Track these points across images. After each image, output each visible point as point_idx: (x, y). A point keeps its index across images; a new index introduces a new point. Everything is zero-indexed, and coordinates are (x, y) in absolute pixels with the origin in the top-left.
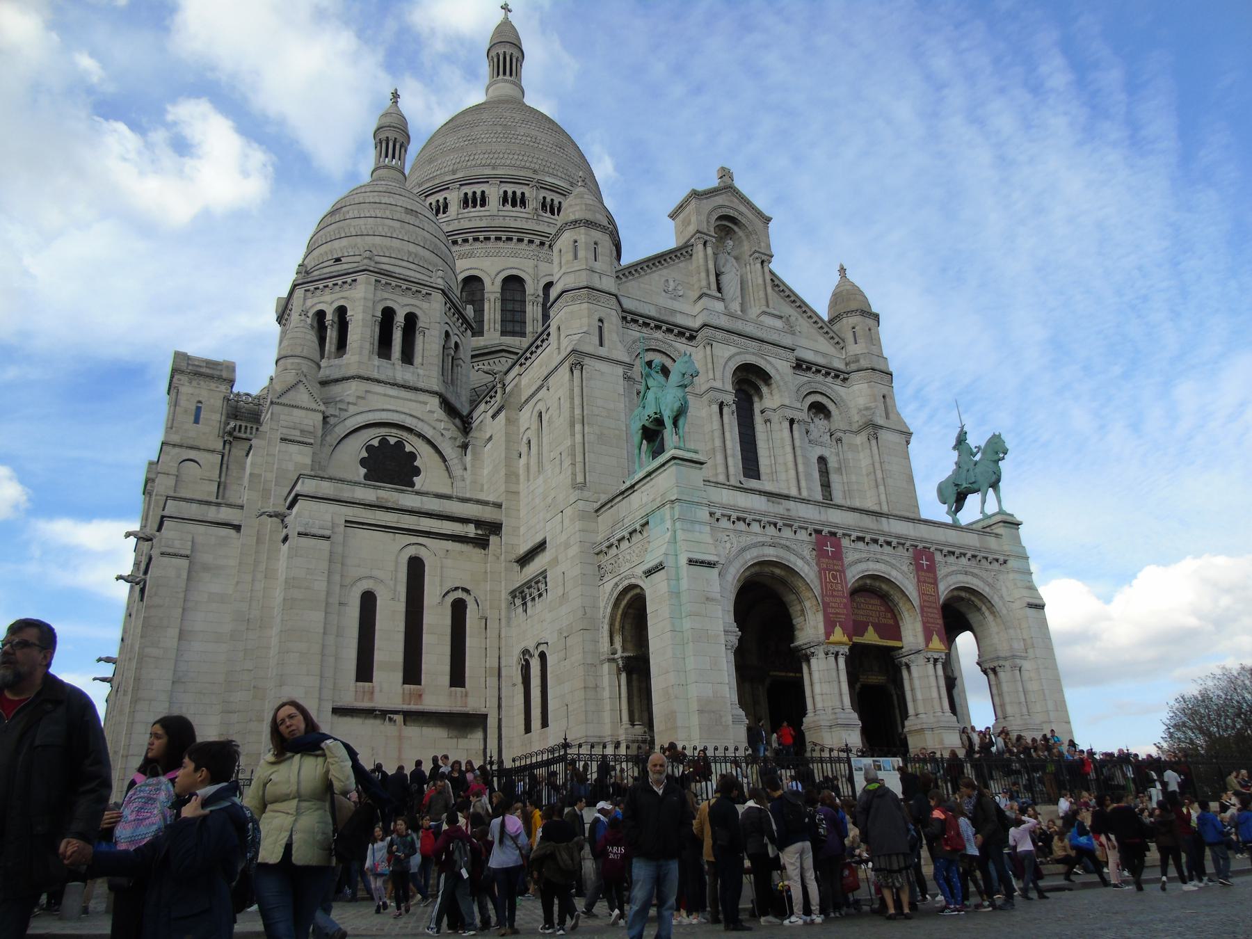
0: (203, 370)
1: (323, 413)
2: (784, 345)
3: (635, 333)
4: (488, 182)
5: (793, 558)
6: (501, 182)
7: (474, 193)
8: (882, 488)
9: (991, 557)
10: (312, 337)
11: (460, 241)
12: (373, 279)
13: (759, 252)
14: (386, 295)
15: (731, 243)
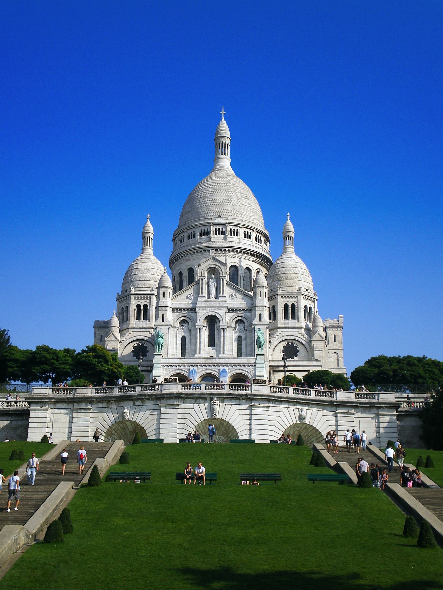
0: (101, 326)
1: (118, 341)
2: (223, 306)
3: (177, 313)
4: (195, 227)
5: (184, 372)
6: (199, 226)
7: (191, 232)
8: (253, 343)
9: (249, 365)
10: (121, 316)
11: (186, 255)
12: (133, 297)
13: (221, 277)
14: (137, 301)
15: (213, 275)
